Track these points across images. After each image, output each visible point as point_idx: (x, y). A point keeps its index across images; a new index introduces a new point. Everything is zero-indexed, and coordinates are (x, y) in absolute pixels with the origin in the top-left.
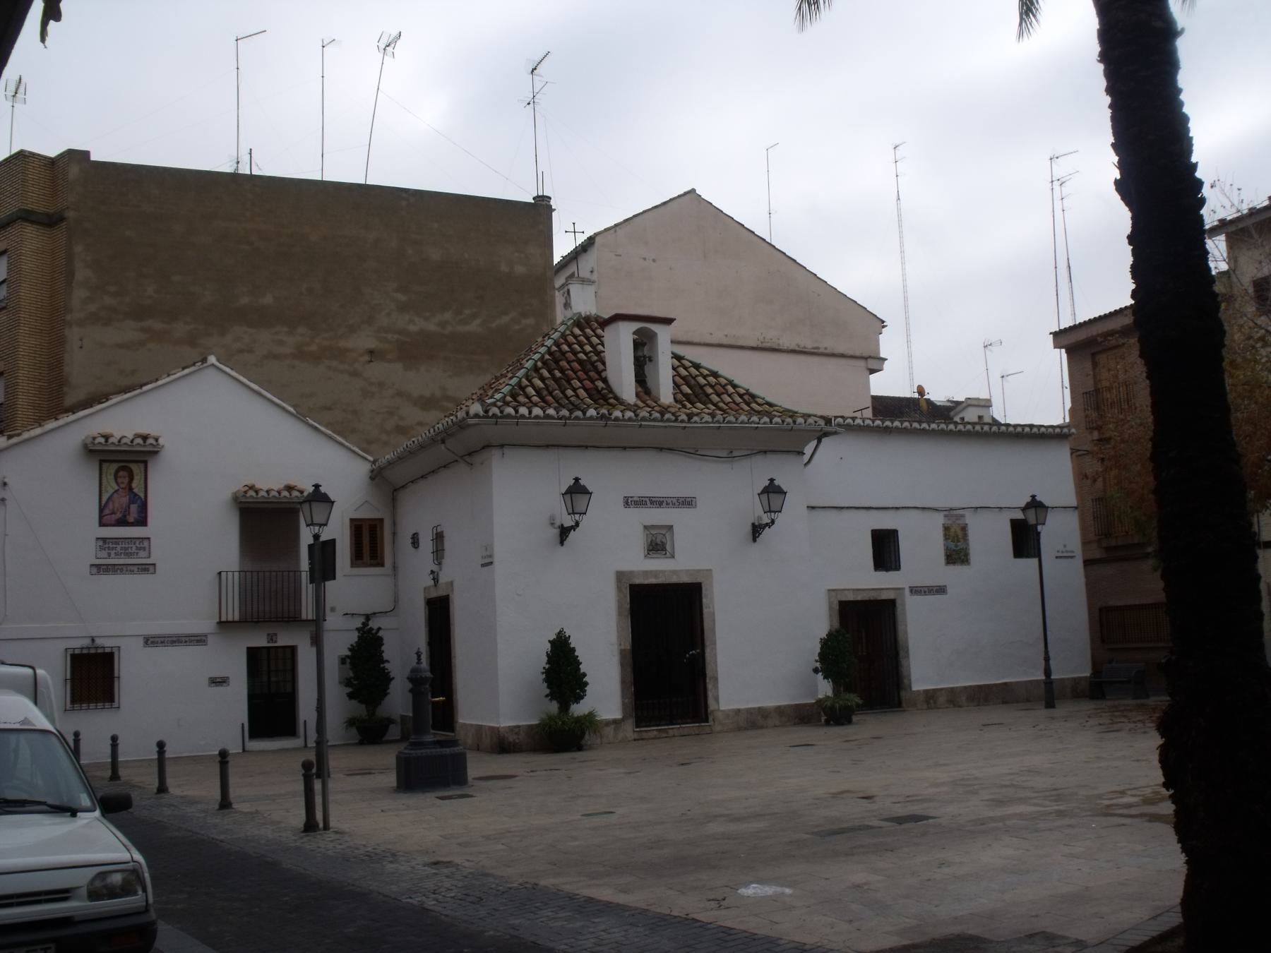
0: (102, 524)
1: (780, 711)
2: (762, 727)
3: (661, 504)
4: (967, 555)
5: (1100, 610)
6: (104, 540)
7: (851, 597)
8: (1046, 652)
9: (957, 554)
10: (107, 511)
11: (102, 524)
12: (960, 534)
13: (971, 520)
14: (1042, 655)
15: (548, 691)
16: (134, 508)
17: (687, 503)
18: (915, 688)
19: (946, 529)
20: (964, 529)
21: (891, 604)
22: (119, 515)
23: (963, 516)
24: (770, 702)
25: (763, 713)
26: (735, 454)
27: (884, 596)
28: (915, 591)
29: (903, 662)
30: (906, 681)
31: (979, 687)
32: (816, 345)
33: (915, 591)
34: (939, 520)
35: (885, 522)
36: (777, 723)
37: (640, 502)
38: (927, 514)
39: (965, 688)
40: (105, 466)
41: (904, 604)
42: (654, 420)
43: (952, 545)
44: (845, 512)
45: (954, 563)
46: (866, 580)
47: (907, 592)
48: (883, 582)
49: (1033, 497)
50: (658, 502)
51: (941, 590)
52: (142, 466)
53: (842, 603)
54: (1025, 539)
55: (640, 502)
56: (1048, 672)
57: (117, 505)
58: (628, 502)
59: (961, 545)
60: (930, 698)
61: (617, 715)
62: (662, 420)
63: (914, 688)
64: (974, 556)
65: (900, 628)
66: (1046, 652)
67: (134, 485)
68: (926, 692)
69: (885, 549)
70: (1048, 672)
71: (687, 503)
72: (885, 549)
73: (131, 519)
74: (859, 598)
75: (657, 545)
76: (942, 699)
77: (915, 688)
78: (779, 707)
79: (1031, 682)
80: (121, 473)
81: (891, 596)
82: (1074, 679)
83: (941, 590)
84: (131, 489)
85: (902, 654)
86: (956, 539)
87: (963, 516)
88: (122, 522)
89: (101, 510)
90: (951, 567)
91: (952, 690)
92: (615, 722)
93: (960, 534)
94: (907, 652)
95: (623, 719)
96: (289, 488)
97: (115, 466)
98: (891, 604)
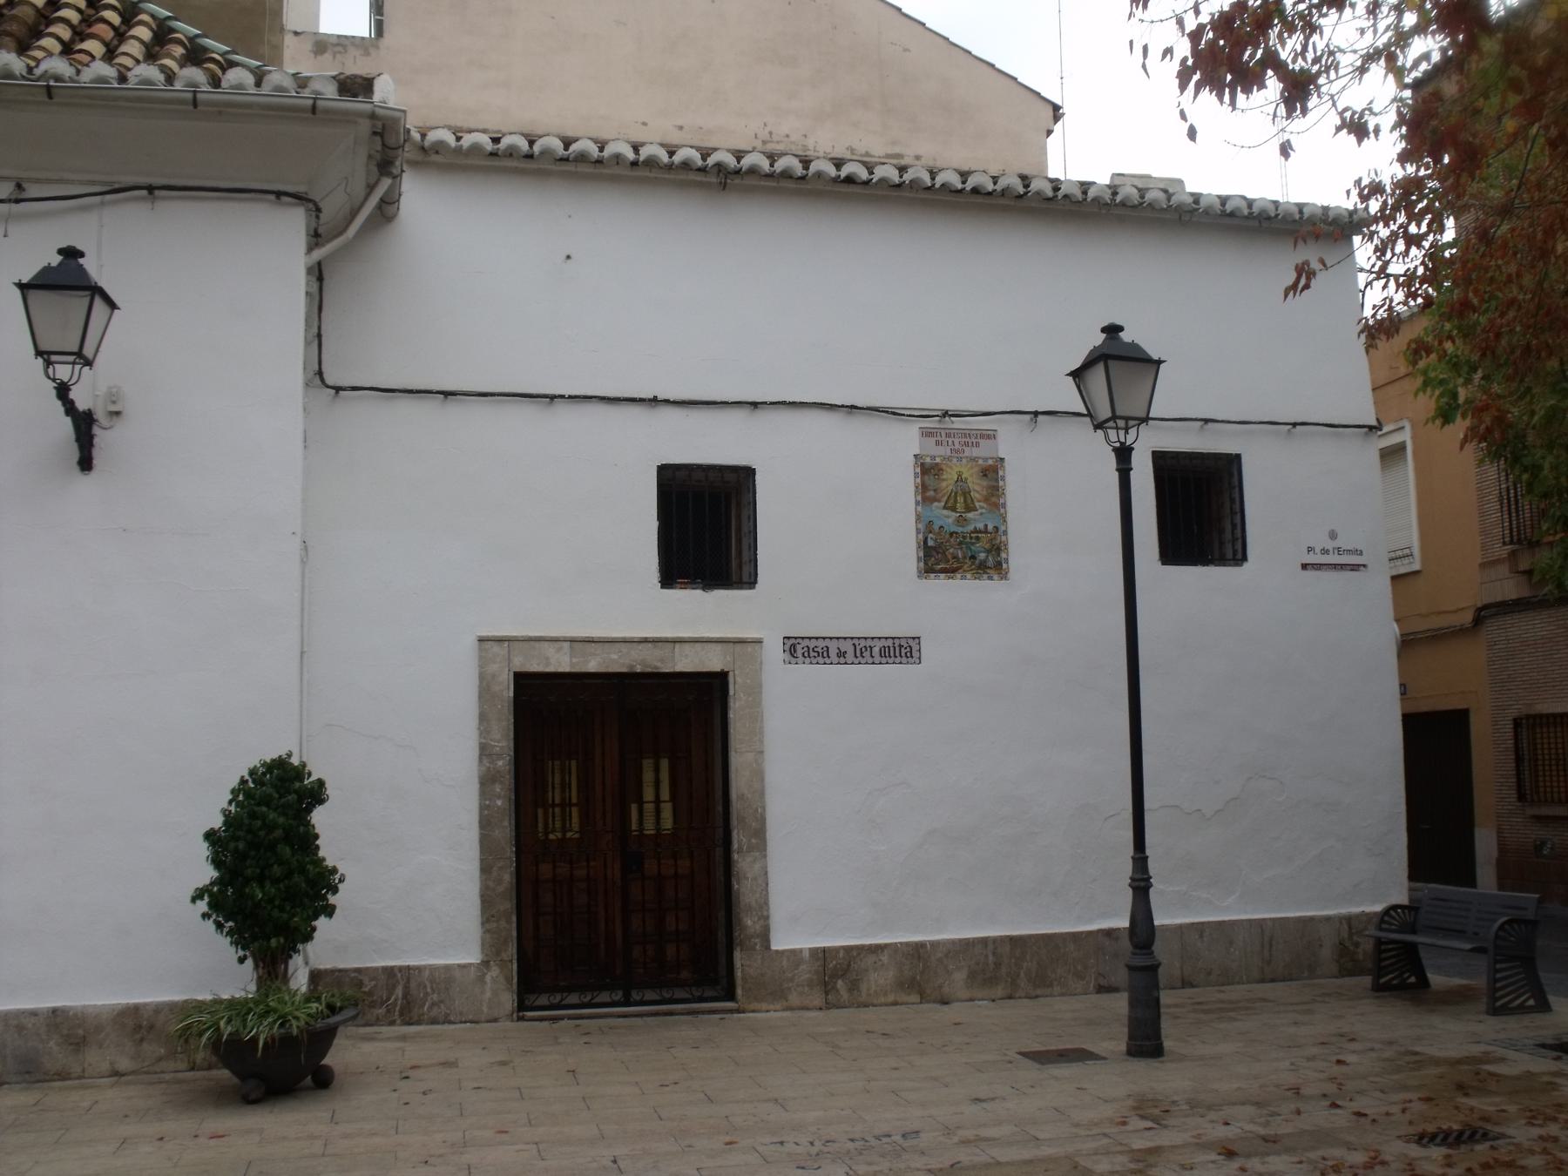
1: (136, 1024)
2: (63, 1076)
4: (997, 549)
5: (1517, 723)
7: (561, 662)
9: (961, 540)
12: (977, 487)
13: (1011, 445)
14: (1127, 868)
15: (208, 874)
18: (782, 941)
19: (928, 471)
20: (992, 472)
23: (990, 436)
24: (97, 992)
25: (71, 1029)
26: (33, 191)
27: (685, 662)
28: (797, 648)
29: (744, 863)
30: (750, 922)
31: (1013, 940)
32: (897, 150)
33: (797, 648)
34: (907, 442)
35: (709, 444)
36: (124, 1064)
38: (858, 423)
39: (967, 945)
41: (756, 690)
43: (947, 519)
44: (563, 411)
45: (950, 571)
46: (625, 609)
47: (774, 651)
48: (685, 624)
49: (1112, 330)
51: (902, 650)
53: (523, 681)
54: (1198, 509)
59: (977, 520)
60: (836, 973)
63: (780, 942)
64: (1017, 555)
65: (739, 760)
68: (823, 954)
69: (705, 524)
72: (705, 524)
74: (593, 666)
76: (879, 979)
77: (782, 941)
78: (136, 1009)
79: (1200, 928)
81: (712, 661)
82: (1349, 920)
83: (902, 650)
85: (738, 838)
86: (961, 500)
87: (990, 436)
90: (939, 583)
91: (917, 952)
93: (977, 487)
94: (760, 833)
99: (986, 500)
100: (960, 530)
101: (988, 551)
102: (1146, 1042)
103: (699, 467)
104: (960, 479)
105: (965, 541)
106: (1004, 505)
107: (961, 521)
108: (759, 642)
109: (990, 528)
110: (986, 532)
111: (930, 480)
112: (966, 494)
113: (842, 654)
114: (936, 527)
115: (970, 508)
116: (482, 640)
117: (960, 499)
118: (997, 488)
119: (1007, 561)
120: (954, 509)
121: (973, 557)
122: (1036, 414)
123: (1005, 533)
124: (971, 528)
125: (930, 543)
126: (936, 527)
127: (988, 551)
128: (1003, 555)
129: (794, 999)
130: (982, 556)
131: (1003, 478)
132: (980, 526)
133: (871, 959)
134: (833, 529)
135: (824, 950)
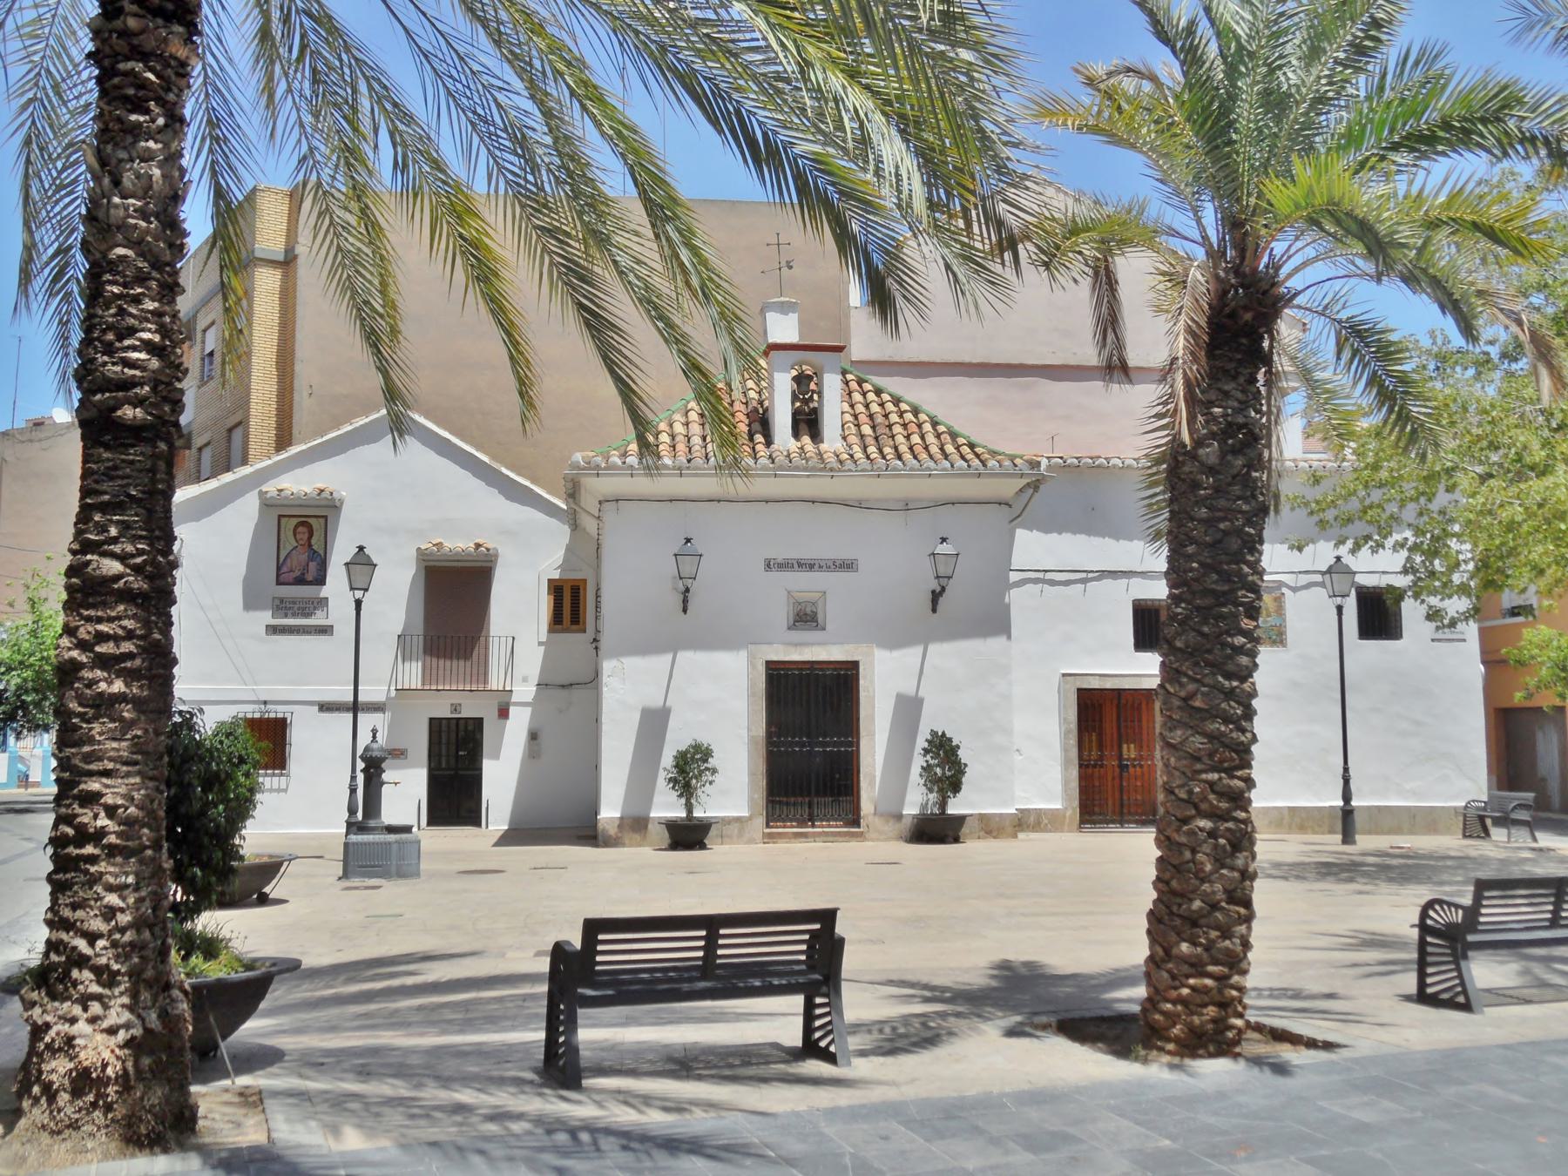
0: (279, 583)
3: (811, 567)
6: (282, 601)
7: (1095, 684)
8: (1346, 770)
10: (285, 569)
11: (279, 583)
16: (313, 565)
17: (847, 566)
22: (297, 573)
37: (785, 566)
40: (284, 520)
42: (797, 468)
52: (322, 521)
55: (785, 566)
56: (1347, 796)
57: (295, 563)
58: (768, 565)
61: (744, 813)
62: (805, 469)
64: (1290, 636)
66: (1346, 770)
67: (313, 541)
70: (1347, 796)
71: (847, 566)
73: (309, 577)
74: (1108, 686)
75: (806, 618)
80: (300, 529)
84: (310, 545)
88: (301, 581)
89: (278, 568)
92: (738, 819)
95: (750, 818)
96: (478, 546)
97: (295, 521)
102: (1348, 838)
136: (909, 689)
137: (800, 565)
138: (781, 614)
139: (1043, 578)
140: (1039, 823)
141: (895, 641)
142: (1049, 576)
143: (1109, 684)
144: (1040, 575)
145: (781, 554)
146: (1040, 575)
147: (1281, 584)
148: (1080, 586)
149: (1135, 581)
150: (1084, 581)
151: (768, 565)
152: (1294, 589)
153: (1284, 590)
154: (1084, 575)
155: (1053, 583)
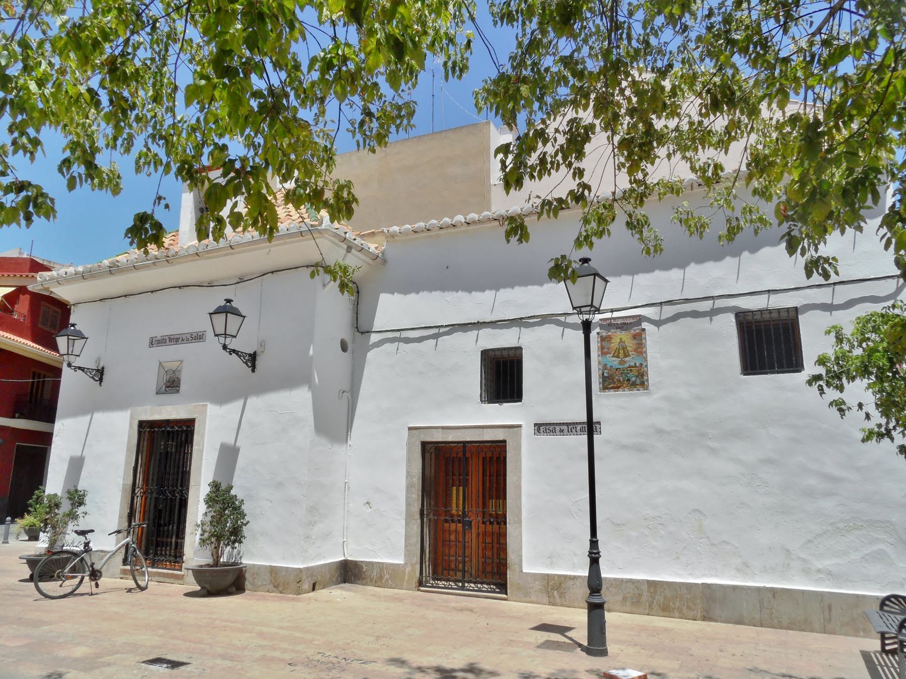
7: (438, 437)
8: (594, 543)
18: (528, 568)
21: (501, 446)
27: (488, 436)
35: (504, 339)
43: (614, 362)
47: (527, 430)
50: (175, 340)
64: (652, 377)
66: (594, 543)
69: (503, 377)
72: (503, 377)
77: (528, 568)
81: (498, 435)
93: (630, 344)
98: (501, 446)
99: (635, 350)
100: (621, 367)
101: (637, 377)
103: (498, 349)
104: (621, 341)
105: (622, 372)
106: (646, 352)
107: (622, 362)
108: (520, 426)
109: (638, 364)
110: (635, 366)
111: (605, 344)
112: (624, 348)
113: (562, 431)
114: (608, 367)
115: (626, 356)
116: (410, 429)
117: (622, 352)
118: (641, 344)
119: (648, 380)
120: (618, 357)
121: (629, 380)
122: (661, 303)
123: (646, 366)
124: (627, 365)
125: (606, 375)
126: (608, 367)
127: (637, 377)
128: (645, 378)
129: (534, 598)
130: (634, 379)
131: (645, 339)
132: (633, 364)
133: (571, 582)
134: (555, 373)
135: (548, 575)
136: (230, 441)
137: (170, 340)
138: (152, 379)
139: (399, 337)
140: (381, 578)
141: (222, 399)
142: (405, 334)
143: (451, 437)
144: (397, 334)
145: (160, 333)
146: (397, 334)
147: (640, 319)
148: (433, 341)
149: (485, 332)
150: (436, 336)
151: (151, 344)
152: (658, 323)
153: (645, 325)
154: (436, 331)
155: (408, 341)
